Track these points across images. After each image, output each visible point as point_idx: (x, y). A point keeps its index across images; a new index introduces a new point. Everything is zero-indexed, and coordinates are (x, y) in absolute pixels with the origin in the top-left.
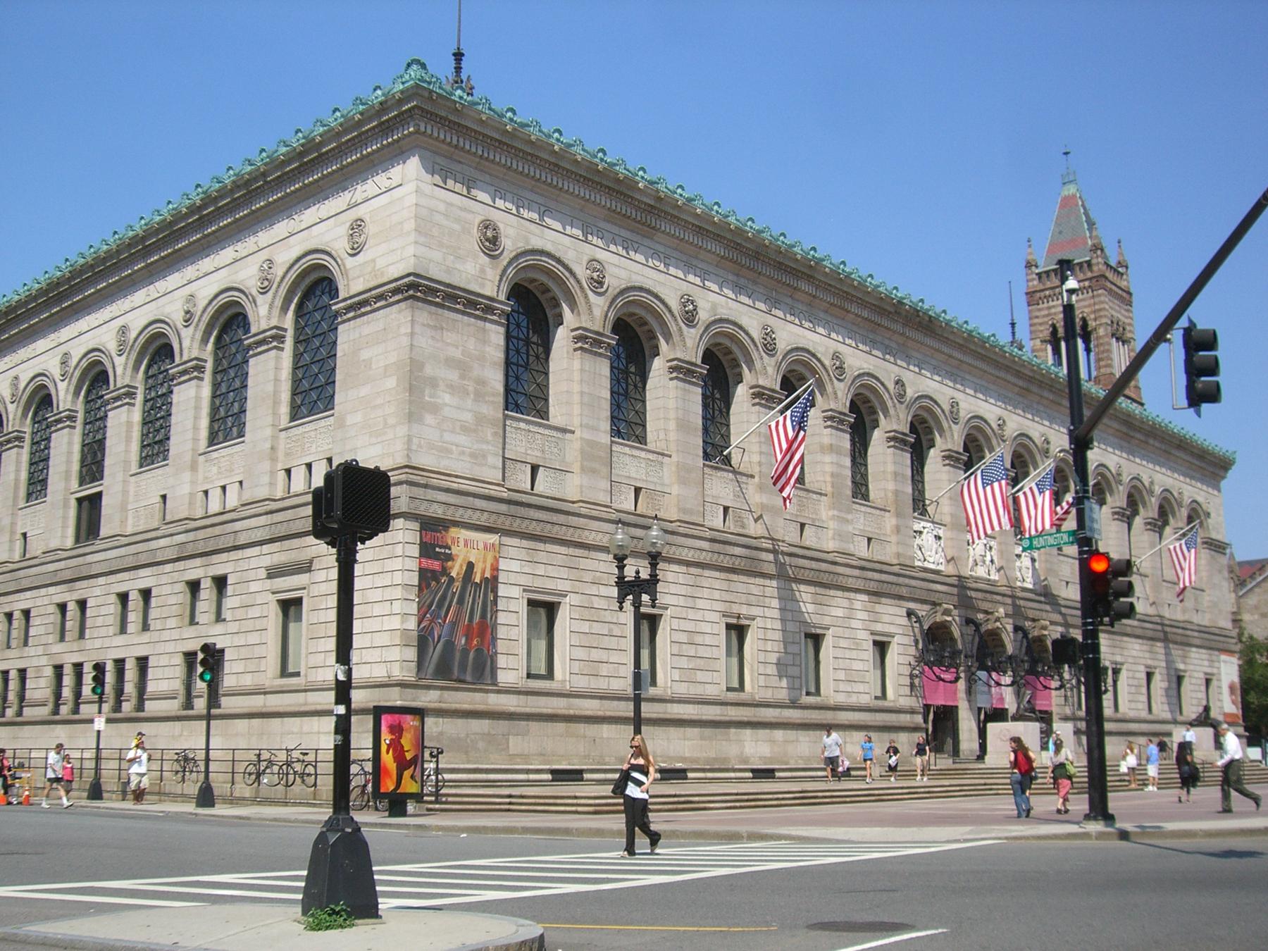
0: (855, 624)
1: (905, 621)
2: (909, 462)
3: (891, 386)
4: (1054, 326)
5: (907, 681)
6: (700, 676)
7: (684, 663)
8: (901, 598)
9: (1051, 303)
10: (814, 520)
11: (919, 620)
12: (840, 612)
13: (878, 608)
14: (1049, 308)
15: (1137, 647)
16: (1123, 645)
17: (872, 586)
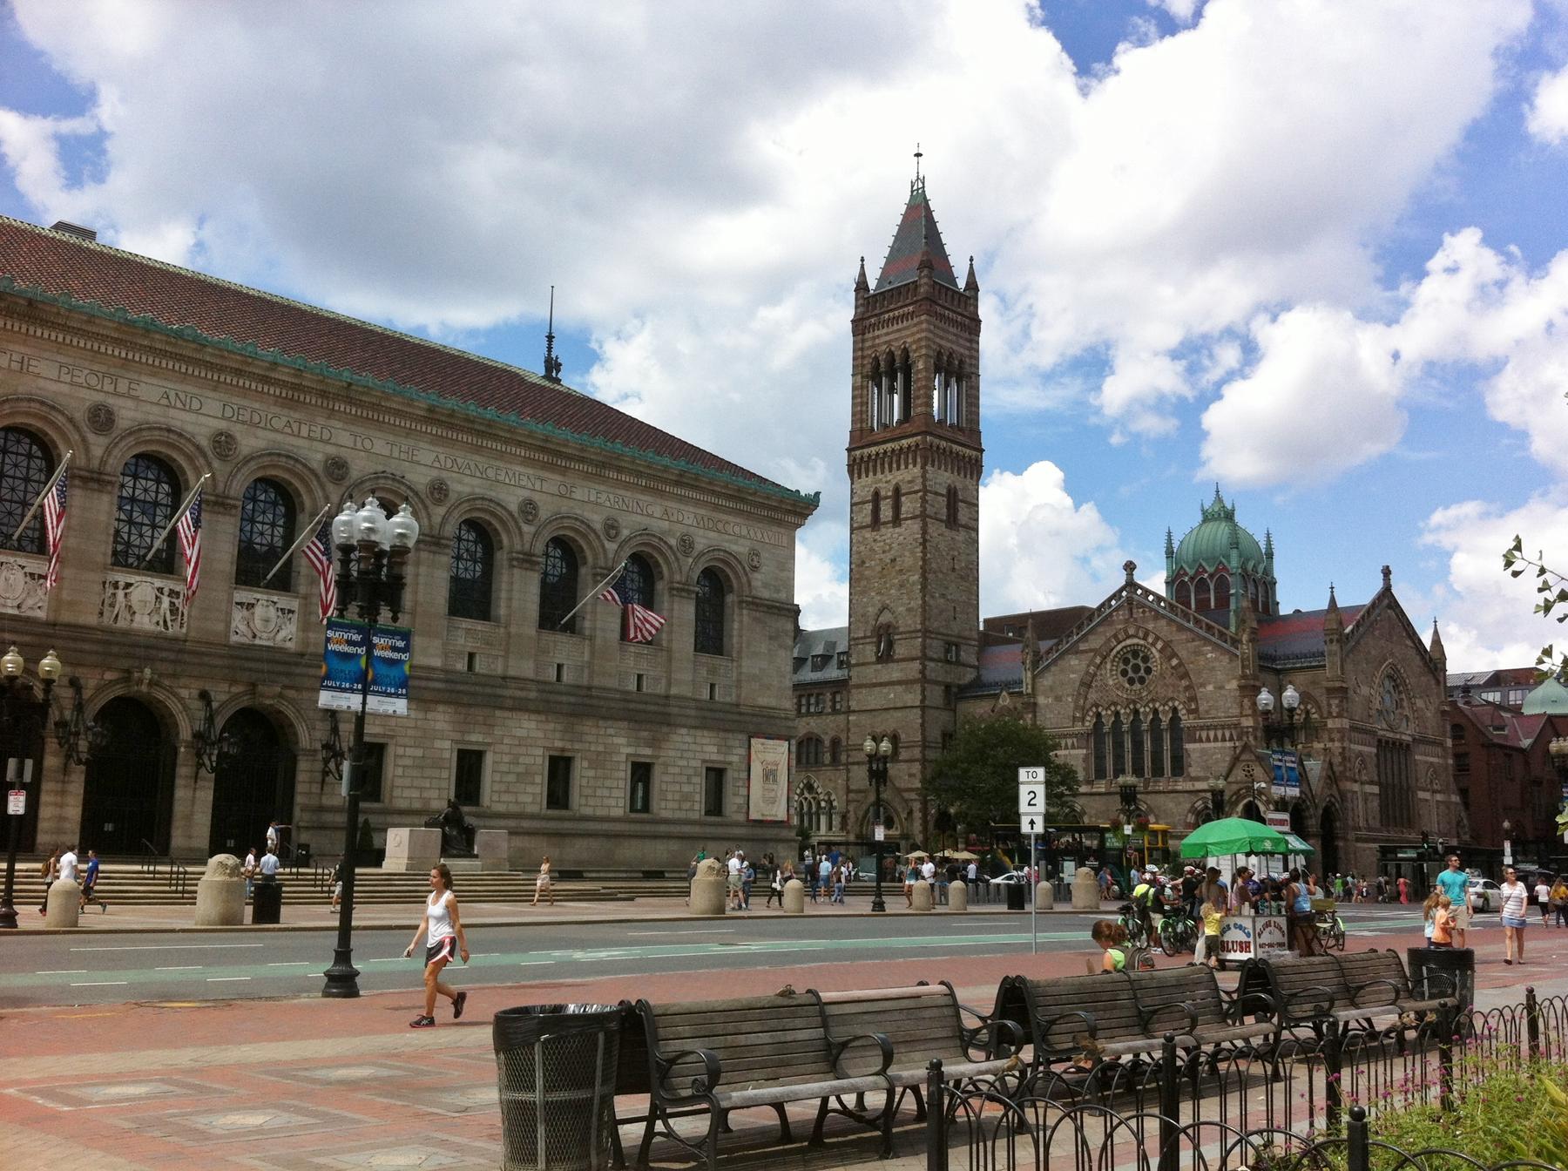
4: (876, 359)
14: (874, 338)
15: (533, 725)
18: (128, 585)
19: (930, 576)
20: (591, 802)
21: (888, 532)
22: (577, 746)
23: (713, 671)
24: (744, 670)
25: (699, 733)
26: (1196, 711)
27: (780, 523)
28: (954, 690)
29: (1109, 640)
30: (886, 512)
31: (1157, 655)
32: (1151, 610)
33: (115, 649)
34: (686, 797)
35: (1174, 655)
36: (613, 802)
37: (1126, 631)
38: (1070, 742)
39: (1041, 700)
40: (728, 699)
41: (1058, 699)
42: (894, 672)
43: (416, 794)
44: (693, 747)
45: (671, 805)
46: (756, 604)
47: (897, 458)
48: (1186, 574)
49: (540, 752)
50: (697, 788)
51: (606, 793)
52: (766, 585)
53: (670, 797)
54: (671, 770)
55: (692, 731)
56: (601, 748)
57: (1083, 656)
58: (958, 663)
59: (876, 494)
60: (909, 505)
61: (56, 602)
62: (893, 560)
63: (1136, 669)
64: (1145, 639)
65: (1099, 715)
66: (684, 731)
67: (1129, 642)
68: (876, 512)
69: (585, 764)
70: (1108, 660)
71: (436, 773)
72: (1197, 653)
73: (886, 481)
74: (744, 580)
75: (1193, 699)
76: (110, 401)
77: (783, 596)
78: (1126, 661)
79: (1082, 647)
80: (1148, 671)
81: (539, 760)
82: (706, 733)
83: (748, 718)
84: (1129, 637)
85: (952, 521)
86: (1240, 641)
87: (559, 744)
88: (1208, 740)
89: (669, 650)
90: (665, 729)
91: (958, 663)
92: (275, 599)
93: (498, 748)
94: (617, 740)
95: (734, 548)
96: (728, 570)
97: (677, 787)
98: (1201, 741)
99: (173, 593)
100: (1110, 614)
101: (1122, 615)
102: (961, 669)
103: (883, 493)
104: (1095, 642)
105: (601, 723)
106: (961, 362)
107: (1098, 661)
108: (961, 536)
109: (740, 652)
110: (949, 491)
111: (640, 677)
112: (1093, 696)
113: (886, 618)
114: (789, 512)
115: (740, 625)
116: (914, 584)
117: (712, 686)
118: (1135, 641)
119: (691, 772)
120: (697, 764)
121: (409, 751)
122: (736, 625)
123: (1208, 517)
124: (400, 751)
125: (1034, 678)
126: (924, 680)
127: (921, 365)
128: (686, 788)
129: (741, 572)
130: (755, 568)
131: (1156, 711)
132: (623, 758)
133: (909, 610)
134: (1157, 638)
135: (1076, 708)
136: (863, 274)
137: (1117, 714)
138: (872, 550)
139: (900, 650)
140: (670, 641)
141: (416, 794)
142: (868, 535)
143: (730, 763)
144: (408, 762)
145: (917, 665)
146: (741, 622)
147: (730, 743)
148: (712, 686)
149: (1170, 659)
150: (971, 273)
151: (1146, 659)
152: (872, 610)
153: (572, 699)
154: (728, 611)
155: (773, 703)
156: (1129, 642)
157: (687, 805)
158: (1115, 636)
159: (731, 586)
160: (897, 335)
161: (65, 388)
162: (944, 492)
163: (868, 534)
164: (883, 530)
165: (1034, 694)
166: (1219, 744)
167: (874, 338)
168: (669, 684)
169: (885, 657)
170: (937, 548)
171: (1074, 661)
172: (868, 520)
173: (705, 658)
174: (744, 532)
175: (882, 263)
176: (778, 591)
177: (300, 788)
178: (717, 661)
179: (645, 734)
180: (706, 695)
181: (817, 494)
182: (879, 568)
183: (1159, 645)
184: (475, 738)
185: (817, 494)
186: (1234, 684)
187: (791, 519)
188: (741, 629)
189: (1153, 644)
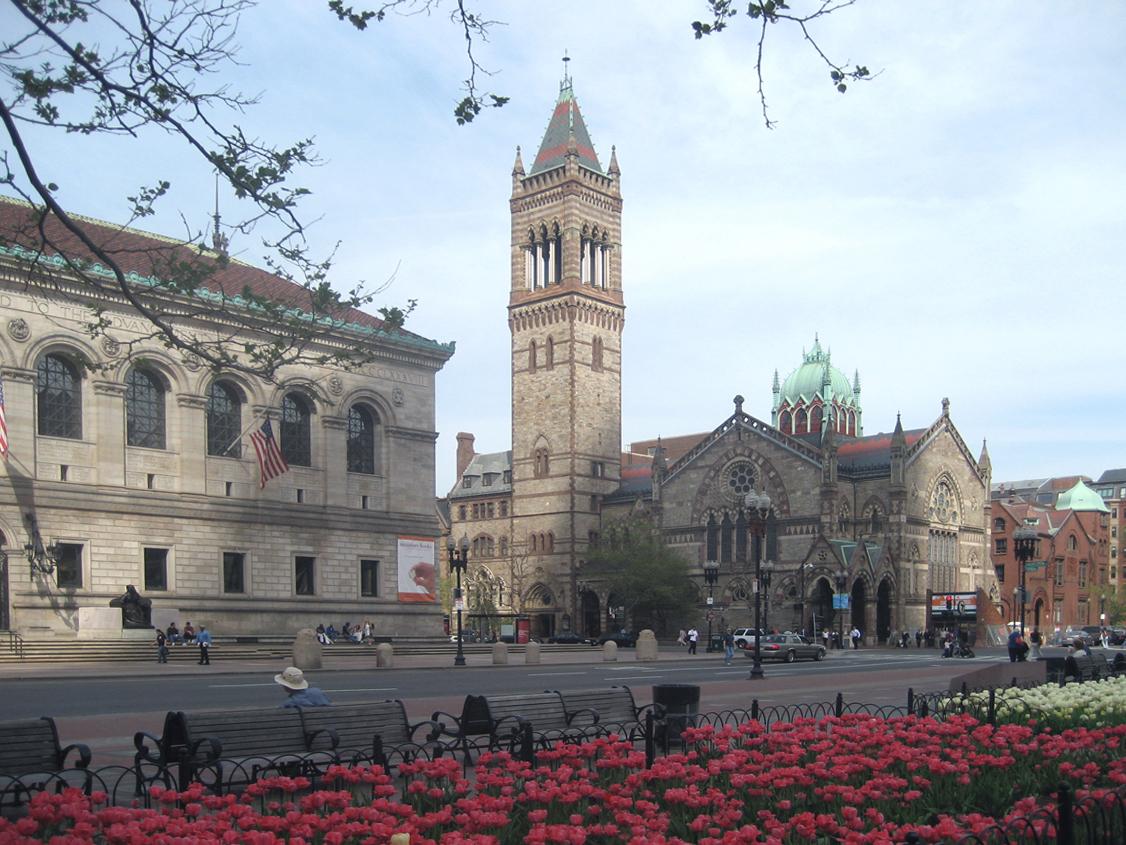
4: (531, 231)
9: (531, 210)
14: (529, 215)
19: (578, 410)
20: (263, 587)
21: (542, 374)
22: (247, 545)
23: (364, 486)
24: (392, 485)
25: (354, 534)
26: (788, 511)
27: (420, 367)
28: (601, 498)
29: (721, 458)
30: (541, 358)
31: (759, 469)
32: (755, 434)
34: (344, 583)
35: (773, 469)
36: (281, 587)
37: (734, 451)
38: (688, 536)
39: (667, 505)
40: (379, 508)
41: (680, 504)
42: (549, 485)
43: (110, 582)
44: (349, 545)
45: (330, 589)
46: (401, 433)
47: (550, 315)
48: (789, 405)
49: (215, 550)
50: (355, 576)
51: (275, 580)
52: (408, 418)
53: (330, 582)
54: (330, 563)
55: (347, 533)
56: (269, 547)
57: (701, 472)
58: (603, 478)
59: (533, 343)
60: (559, 353)
62: (547, 397)
63: (742, 479)
64: (750, 457)
65: (712, 516)
66: (340, 533)
67: (737, 459)
68: (533, 358)
69: (255, 559)
70: (720, 474)
71: (127, 566)
72: (791, 467)
73: (541, 333)
74: (389, 413)
75: (786, 502)
77: (425, 426)
78: (734, 474)
79: (700, 463)
81: (215, 556)
82: (360, 534)
83: (397, 523)
84: (736, 455)
85: (597, 364)
86: (823, 457)
87: (233, 544)
88: (796, 533)
89: (325, 471)
90: (323, 532)
91: (603, 478)
93: (179, 547)
94: (281, 541)
95: (379, 388)
96: (376, 407)
97: (337, 576)
98: (790, 534)
100: (722, 438)
101: (733, 438)
102: (605, 482)
103: (538, 343)
104: (710, 460)
105: (267, 527)
106: (605, 234)
107: (712, 474)
108: (606, 376)
109: (388, 471)
110: (595, 340)
111: (300, 492)
113: (542, 443)
114: (428, 358)
115: (386, 450)
116: (564, 416)
117: (365, 498)
118: (742, 458)
119: (349, 564)
120: (354, 558)
121: (102, 550)
122: (384, 450)
124: (95, 550)
125: (661, 487)
126: (572, 490)
127: (568, 236)
128: (344, 576)
129: (386, 408)
130: (399, 404)
132: (289, 554)
133: (561, 437)
135: (695, 510)
136: (519, 161)
138: (530, 389)
139: (554, 468)
140: (325, 463)
141: (110, 582)
142: (526, 377)
143: (382, 557)
144: (104, 558)
145: (567, 480)
146: (388, 447)
147: (381, 541)
148: (365, 498)
150: (614, 160)
151: (750, 472)
152: (530, 438)
153: (241, 510)
154: (376, 439)
155: (418, 510)
156: (737, 459)
157: (344, 589)
159: (378, 419)
160: (548, 212)
162: (591, 341)
163: (526, 376)
164: (539, 372)
165: (660, 501)
166: (802, 536)
167: (529, 215)
168: (326, 497)
169: (542, 474)
170: (584, 388)
171: (693, 475)
172: (527, 365)
173: (356, 477)
174: (388, 375)
175: (536, 151)
176: (420, 422)
177: (11, 578)
178: (368, 479)
180: (359, 505)
181: (453, 343)
182: (536, 404)
184: (158, 541)
185: (453, 343)
186: (817, 490)
187: (429, 364)
188: (388, 453)
189: (756, 461)
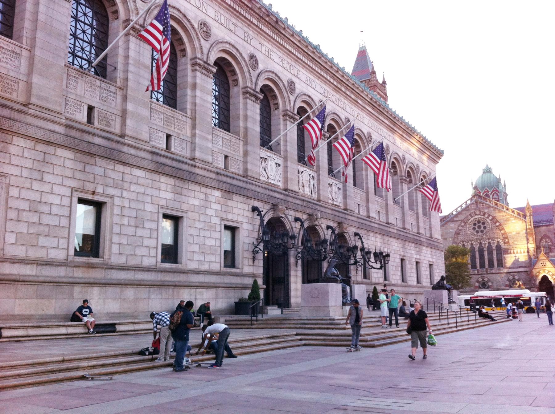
0: (209, 212)
1: (249, 214)
2: (258, 111)
3: (247, 58)
5: (251, 256)
6: (42, 241)
7: (23, 228)
8: (249, 198)
10: (179, 134)
11: (260, 214)
12: (197, 202)
13: (230, 203)
16: (389, 242)
17: (225, 186)
18: (302, 172)
33: (305, 204)
61: (286, 180)
76: (295, 80)
80: (485, 228)
92: (337, 183)
99: (313, 178)
112: (461, 238)
120: (428, 263)
123: (484, 172)
131: (489, 243)
134: (489, 215)
137: (472, 244)
149: (495, 223)
158: (470, 215)
161: (281, 69)
179: (417, 249)
183: (490, 218)
